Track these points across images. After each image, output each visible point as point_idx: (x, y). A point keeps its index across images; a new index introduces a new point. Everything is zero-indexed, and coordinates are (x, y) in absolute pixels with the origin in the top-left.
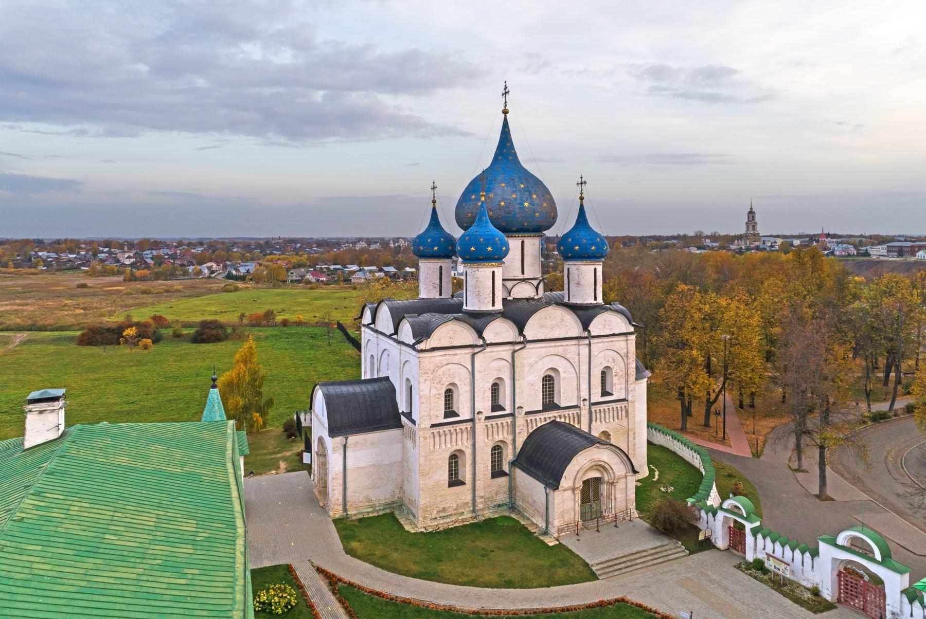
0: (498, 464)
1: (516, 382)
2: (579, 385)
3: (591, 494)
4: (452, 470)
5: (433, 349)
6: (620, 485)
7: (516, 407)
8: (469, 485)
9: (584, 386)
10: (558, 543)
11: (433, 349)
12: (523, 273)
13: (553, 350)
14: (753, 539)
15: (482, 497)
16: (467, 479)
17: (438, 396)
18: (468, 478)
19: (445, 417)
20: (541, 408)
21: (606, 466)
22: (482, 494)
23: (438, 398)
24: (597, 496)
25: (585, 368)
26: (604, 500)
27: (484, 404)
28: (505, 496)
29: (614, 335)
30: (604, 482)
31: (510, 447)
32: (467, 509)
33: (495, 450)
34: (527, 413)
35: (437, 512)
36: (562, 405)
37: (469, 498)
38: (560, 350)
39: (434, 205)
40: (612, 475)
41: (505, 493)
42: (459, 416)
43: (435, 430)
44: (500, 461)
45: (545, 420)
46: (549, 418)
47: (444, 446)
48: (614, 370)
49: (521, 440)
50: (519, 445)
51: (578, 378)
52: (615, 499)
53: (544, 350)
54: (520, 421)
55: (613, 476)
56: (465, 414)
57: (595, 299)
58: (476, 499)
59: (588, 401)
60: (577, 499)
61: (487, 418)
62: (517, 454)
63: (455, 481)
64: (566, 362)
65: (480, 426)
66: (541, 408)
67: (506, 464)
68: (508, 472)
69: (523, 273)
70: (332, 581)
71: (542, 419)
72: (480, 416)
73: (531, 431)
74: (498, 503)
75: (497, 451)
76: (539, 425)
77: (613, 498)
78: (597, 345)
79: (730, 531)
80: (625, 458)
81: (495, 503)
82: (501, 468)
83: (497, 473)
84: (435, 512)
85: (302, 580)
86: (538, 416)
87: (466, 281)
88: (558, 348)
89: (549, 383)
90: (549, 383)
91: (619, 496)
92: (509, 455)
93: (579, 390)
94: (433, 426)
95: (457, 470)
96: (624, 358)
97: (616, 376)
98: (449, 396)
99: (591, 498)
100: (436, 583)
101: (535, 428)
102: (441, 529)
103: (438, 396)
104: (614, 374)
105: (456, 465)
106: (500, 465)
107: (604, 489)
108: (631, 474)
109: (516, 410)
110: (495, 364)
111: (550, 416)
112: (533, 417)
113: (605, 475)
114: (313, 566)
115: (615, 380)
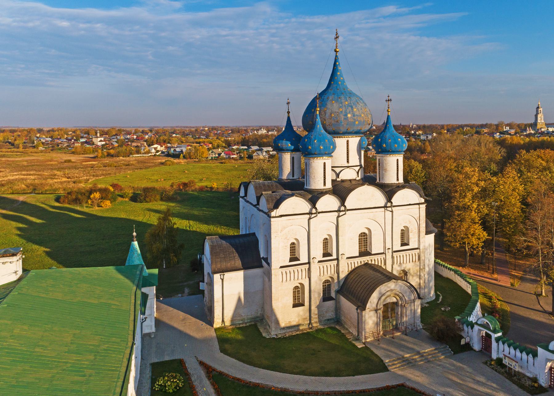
0: (328, 292)
4: (296, 296)
5: (281, 216)
7: (340, 254)
10: (364, 346)
11: (281, 216)
12: (348, 162)
14: (496, 344)
17: (285, 247)
19: (290, 261)
20: (358, 255)
23: (285, 249)
27: (317, 252)
33: (325, 283)
34: (348, 258)
36: (373, 253)
39: (289, 115)
41: (332, 311)
42: (299, 260)
45: (361, 263)
56: (304, 258)
57: (398, 180)
58: (312, 315)
59: (391, 250)
61: (320, 262)
62: (341, 285)
66: (358, 255)
67: (333, 292)
68: (334, 297)
69: (348, 162)
70: (209, 371)
73: (350, 269)
74: (328, 318)
79: (483, 338)
81: (326, 318)
85: (189, 370)
87: (306, 169)
92: (334, 288)
94: (281, 267)
98: (293, 247)
100: (278, 373)
101: (353, 267)
102: (287, 335)
103: (285, 247)
114: (198, 361)
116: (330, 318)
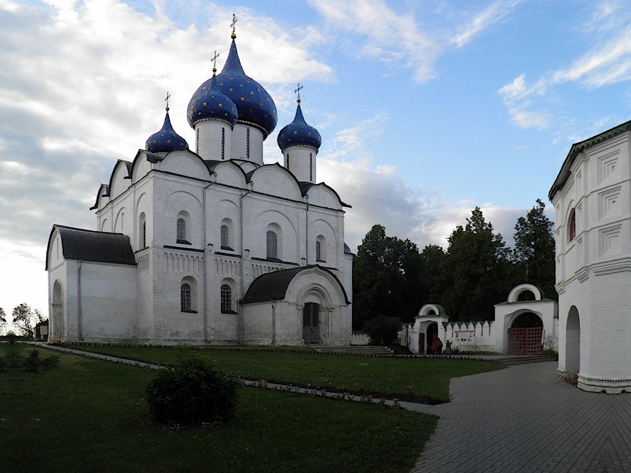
0: (227, 304)
1: (244, 226)
2: (298, 245)
3: (311, 318)
6: (336, 313)
7: (244, 249)
8: (200, 315)
9: (303, 247)
12: (248, 157)
13: (275, 207)
15: (213, 329)
16: (199, 308)
18: (199, 307)
21: (324, 291)
22: (213, 326)
24: (316, 322)
25: (303, 230)
26: (322, 326)
27: (215, 238)
28: (234, 334)
29: (327, 208)
30: (322, 308)
31: (239, 287)
32: (199, 338)
33: (224, 289)
34: (253, 258)
35: (171, 334)
37: (201, 327)
38: (281, 208)
39: (167, 112)
40: (329, 301)
41: (234, 330)
43: (169, 251)
44: (229, 301)
45: (269, 270)
46: (273, 268)
47: (176, 270)
48: (327, 241)
49: (248, 281)
50: (247, 287)
51: (298, 238)
52: (332, 325)
53: (268, 204)
54: (247, 264)
55: (330, 303)
58: (208, 329)
60: (300, 317)
61: (217, 253)
63: (186, 307)
64: (286, 220)
65: (211, 259)
68: (236, 311)
71: (266, 268)
72: (210, 247)
73: (256, 277)
75: (226, 292)
76: (264, 273)
77: (330, 325)
78: (314, 214)
80: (340, 288)
81: (225, 339)
82: (230, 307)
83: (226, 309)
84: (169, 334)
86: (264, 264)
88: (282, 206)
89: (272, 239)
90: (272, 239)
91: (334, 323)
92: (237, 294)
93: (298, 250)
95: (189, 300)
96: (336, 232)
97: (328, 245)
99: (311, 322)
104: (327, 244)
105: (189, 296)
106: (229, 305)
107: (322, 316)
108: (345, 304)
109: (244, 252)
110: (225, 204)
111: (274, 266)
112: (258, 263)
113: (324, 301)
115: (328, 249)
116: (230, 339)
